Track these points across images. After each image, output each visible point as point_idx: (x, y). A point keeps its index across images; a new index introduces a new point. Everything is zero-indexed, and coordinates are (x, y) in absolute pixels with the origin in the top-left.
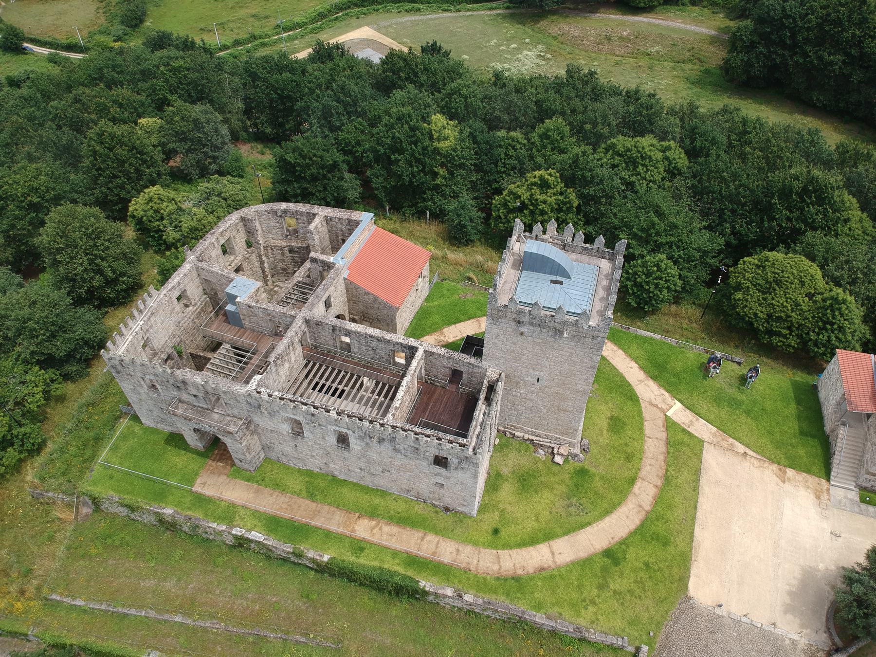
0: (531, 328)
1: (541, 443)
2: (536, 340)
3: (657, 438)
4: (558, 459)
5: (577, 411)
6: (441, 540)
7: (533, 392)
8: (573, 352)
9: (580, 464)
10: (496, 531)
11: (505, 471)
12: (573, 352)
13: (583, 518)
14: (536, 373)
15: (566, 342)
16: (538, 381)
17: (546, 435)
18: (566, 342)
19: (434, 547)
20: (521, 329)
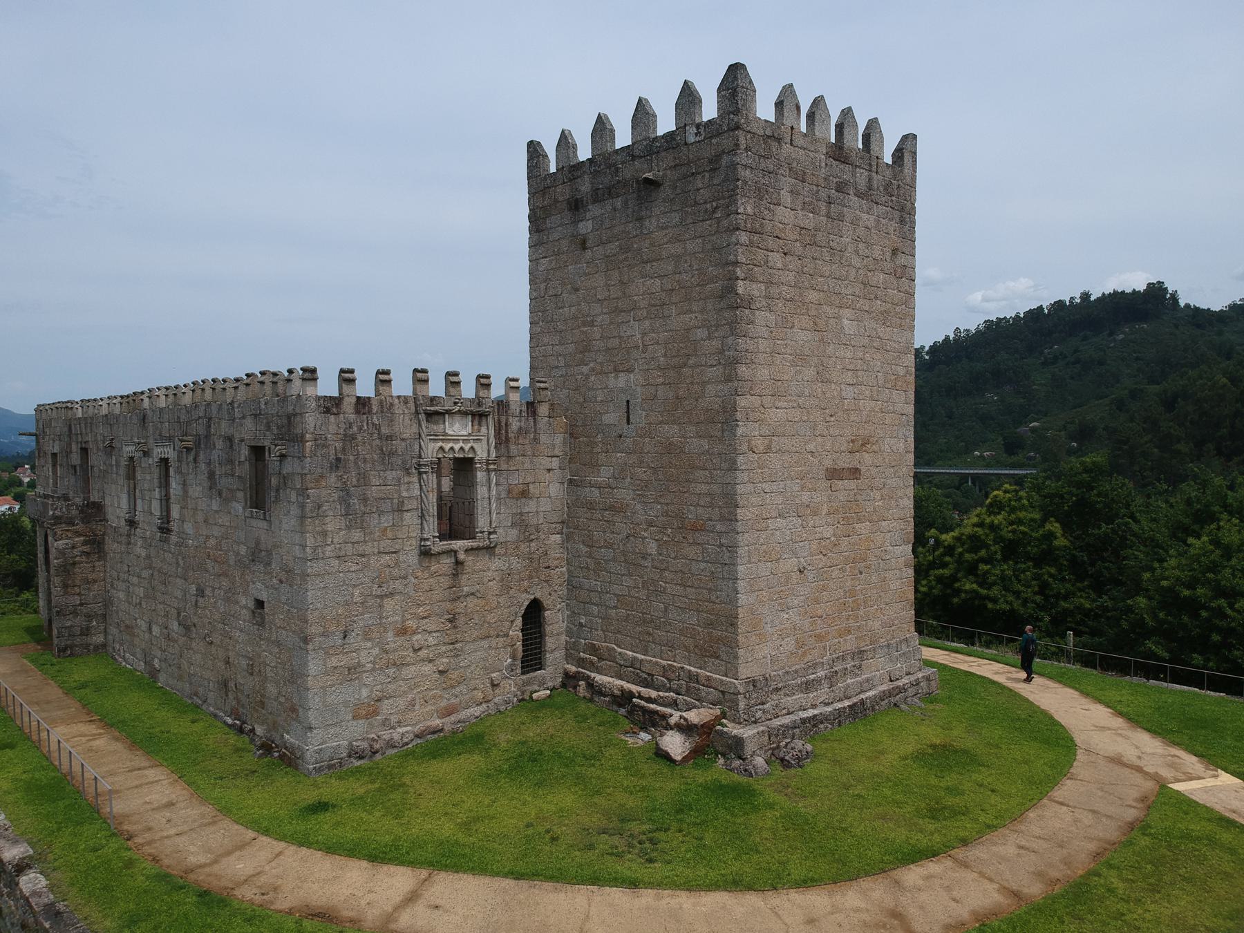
1: (652, 706)
3: (1094, 812)
4: (675, 744)
5: (722, 519)
6: (164, 782)
9: (743, 779)
10: (320, 807)
11: (503, 738)
13: (631, 866)
17: (665, 671)
19: (137, 783)
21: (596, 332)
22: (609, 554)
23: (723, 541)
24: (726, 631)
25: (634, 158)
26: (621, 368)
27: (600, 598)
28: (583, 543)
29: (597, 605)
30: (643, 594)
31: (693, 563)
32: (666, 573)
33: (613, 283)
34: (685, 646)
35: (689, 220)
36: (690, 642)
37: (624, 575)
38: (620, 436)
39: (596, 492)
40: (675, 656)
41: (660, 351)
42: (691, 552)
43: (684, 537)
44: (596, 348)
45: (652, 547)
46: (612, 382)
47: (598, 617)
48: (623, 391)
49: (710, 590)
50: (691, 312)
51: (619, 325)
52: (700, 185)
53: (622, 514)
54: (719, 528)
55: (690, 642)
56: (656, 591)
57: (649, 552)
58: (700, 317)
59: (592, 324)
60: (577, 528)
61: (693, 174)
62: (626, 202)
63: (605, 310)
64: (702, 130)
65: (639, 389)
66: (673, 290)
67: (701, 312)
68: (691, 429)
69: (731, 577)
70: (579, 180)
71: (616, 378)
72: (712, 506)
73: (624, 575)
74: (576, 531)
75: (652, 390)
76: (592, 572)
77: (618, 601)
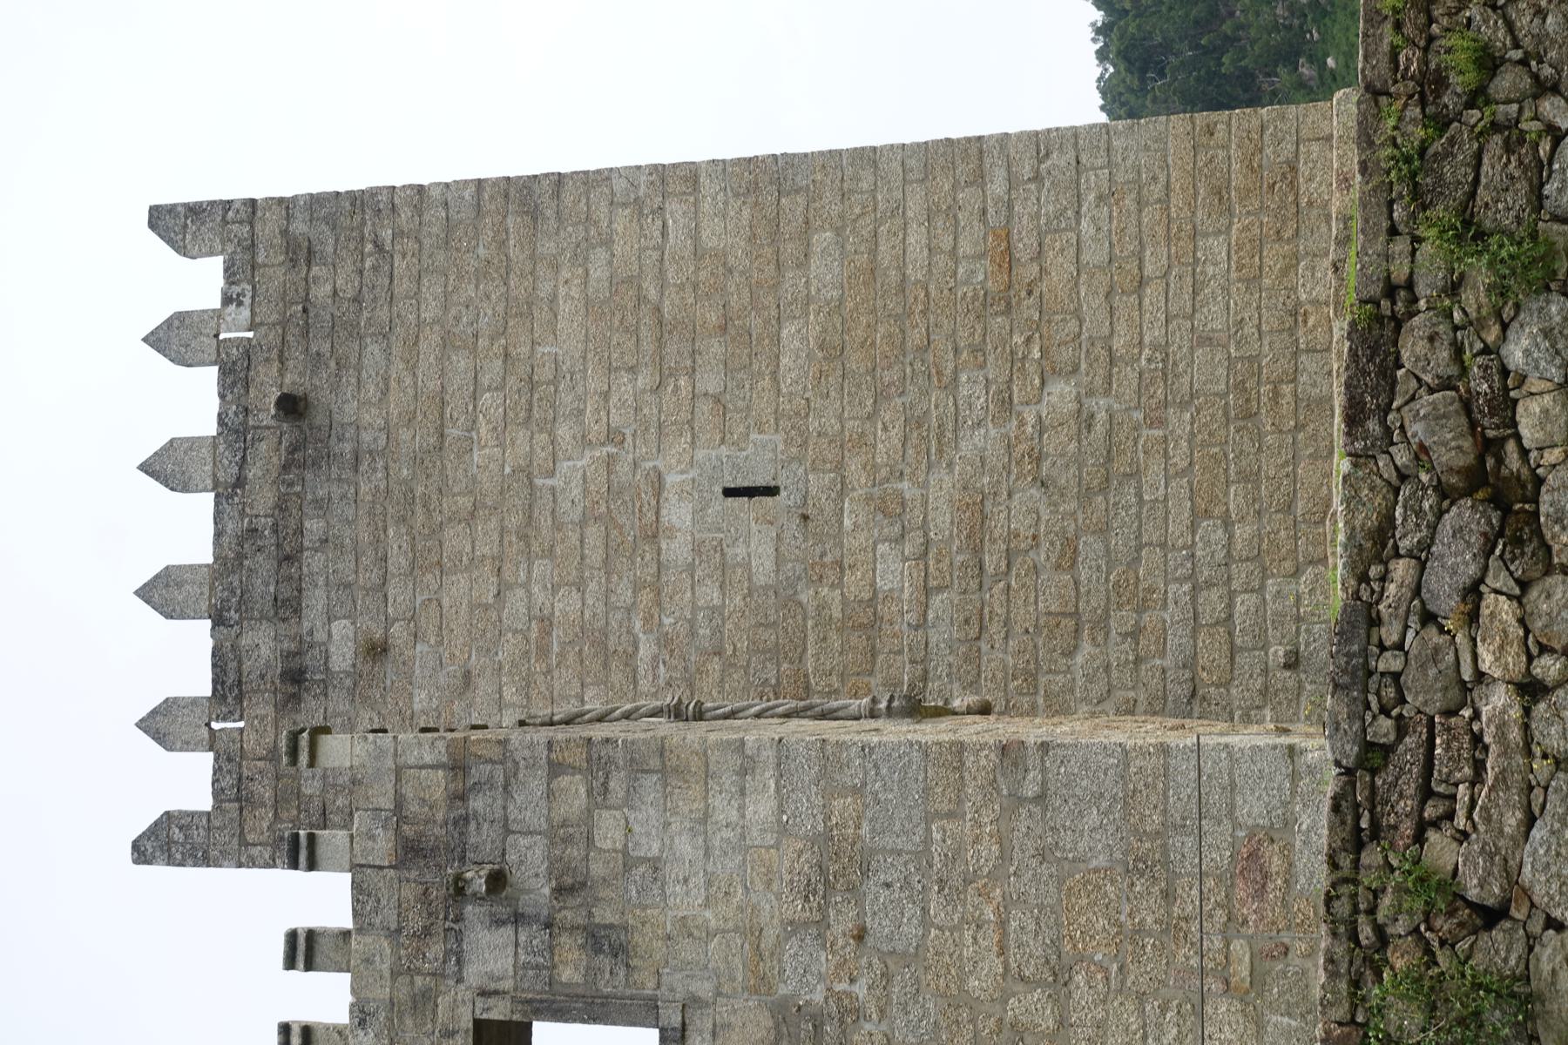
0: (316, 601)
2: (398, 560)
5: (979, 178)
7: (888, 508)
8: (430, 341)
12: (430, 341)
14: (678, 513)
15: (371, 391)
16: (771, 491)
18: (371, 391)
20: (342, 656)
21: (566, 605)
22: (1089, 546)
23: (1027, 172)
24: (1226, 147)
25: (240, 482)
26: (651, 516)
27: (1209, 584)
28: (1070, 653)
29: (1232, 595)
30: (1180, 422)
31: (1085, 258)
32: (1118, 344)
33: (468, 548)
34: (1285, 272)
35: (383, 314)
36: (1273, 256)
37: (1139, 495)
38: (805, 518)
39: (937, 600)
40: (1315, 302)
41: (625, 388)
42: (1060, 267)
43: (1030, 293)
44: (600, 608)
45: (1061, 392)
46: (677, 549)
47: (1262, 587)
48: (699, 512)
49: (1139, 202)
50: (553, 299)
51: (558, 526)
52: (328, 288)
53: (988, 505)
54: (997, 187)
55: (1273, 256)
56: (1165, 375)
57: (1073, 406)
58: (565, 274)
59: (547, 623)
60: (1031, 677)
61: (305, 310)
62: (322, 505)
63: (523, 576)
64: (236, 289)
65: (700, 454)
66: (506, 355)
67: (556, 268)
68: (792, 281)
69: (1103, 145)
70: (247, 665)
71: (671, 532)
72: (952, 212)
73: (1139, 495)
74: (1043, 680)
75: (704, 407)
76: (1146, 617)
77: (1207, 514)
